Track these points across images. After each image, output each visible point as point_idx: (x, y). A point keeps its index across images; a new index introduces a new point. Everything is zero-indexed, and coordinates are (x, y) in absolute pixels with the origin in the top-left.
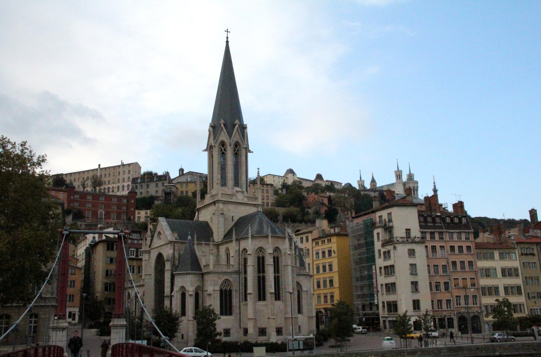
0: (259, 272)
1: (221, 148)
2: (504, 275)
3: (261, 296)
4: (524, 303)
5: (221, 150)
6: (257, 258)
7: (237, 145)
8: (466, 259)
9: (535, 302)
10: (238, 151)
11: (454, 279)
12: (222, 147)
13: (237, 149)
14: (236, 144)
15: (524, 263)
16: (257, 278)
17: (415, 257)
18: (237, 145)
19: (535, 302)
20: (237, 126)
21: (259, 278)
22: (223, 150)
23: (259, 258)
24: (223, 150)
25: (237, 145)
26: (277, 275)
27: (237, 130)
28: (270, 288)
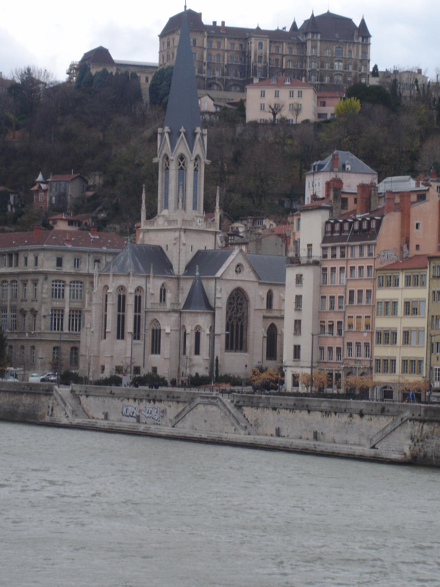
0: (119, 310)
1: (179, 162)
2: (407, 312)
3: (121, 334)
4: (423, 358)
5: (180, 165)
6: (117, 296)
7: (183, 157)
8: (365, 286)
9: (438, 357)
10: (184, 165)
11: (349, 317)
12: (180, 162)
13: (182, 163)
14: (182, 157)
15: (434, 292)
16: (116, 316)
17: (302, 286)
18: (182, 157)
19: (438, 357)
20: (182, 134)
21: (119, 316)
22: (182, 165)
23: (119, 297)
24: (182, 165)
25: (182, 157)
26: (121, 313)
27: (182, 138)
28: (129, 327)
